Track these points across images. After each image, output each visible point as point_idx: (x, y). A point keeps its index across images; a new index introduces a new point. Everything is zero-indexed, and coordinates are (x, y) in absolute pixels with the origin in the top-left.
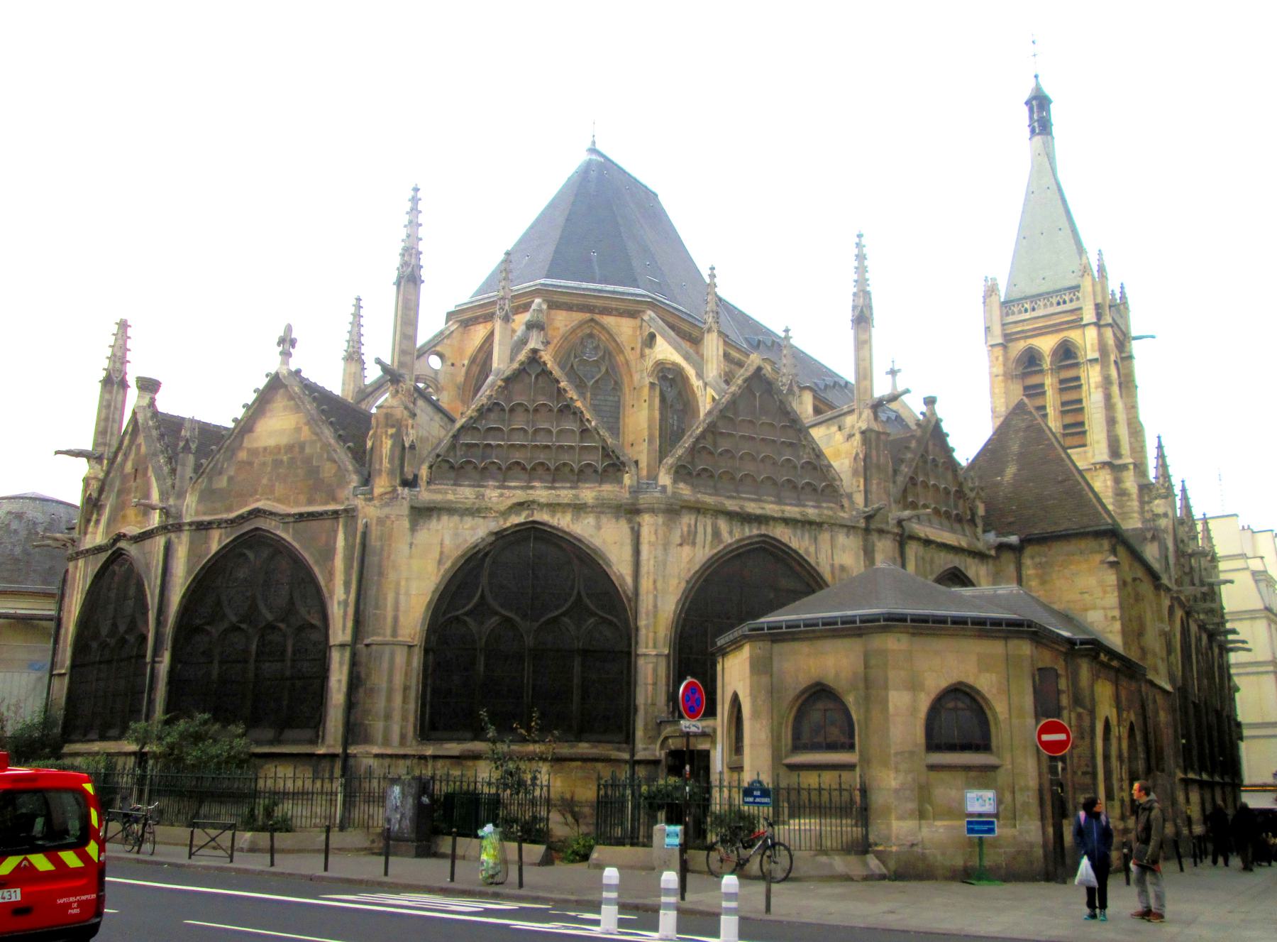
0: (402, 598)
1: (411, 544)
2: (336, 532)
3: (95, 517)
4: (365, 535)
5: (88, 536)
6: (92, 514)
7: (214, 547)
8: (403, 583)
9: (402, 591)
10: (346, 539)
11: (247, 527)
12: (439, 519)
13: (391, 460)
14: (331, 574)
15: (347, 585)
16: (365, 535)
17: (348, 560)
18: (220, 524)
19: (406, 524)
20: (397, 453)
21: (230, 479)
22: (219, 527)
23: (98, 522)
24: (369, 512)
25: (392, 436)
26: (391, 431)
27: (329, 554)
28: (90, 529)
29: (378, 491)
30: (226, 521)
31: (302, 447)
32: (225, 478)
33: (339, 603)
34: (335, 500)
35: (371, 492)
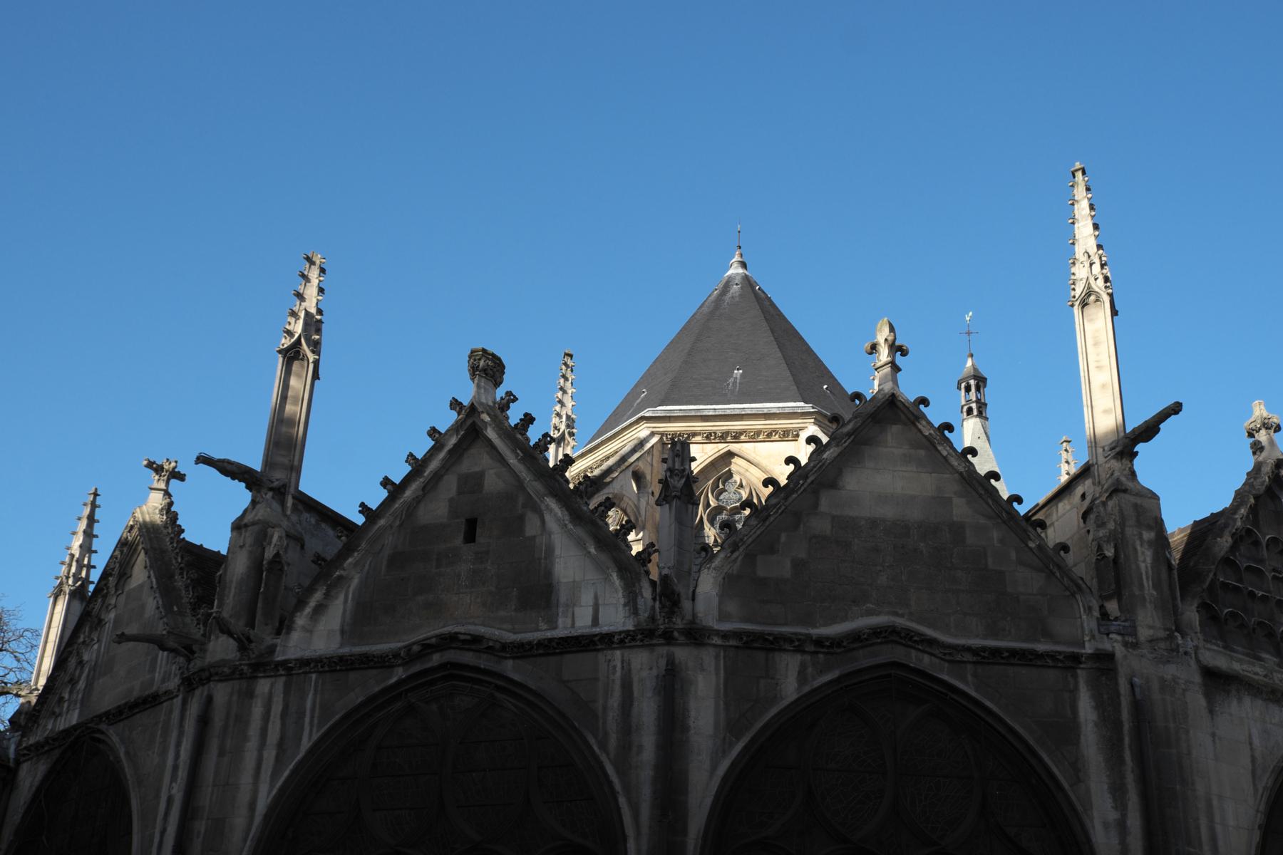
0: (1219, 828)
1: (1213, 735)
2: (1074, 692)
3: (318, 596)
4: (1138, 708)
5: (295, 636)
6: (310, 590)
7: (790, 689)
8: (1215, 802)
9: (1217, 819)
10: (1099, 705)
11: (864, 659)
12: (1240, 700)
13: (1157, 586)
14: (1077, 770)
15: (1118, 791)
16: (1138, 708)
17: (1112, 747)
18: (797, 644)
19: (1202, 702)
20: (1164, 575)
21: (798, 565)
22: (799, 650)
23: (320, 609)
24: (1136, 666)
25: (1150, 543)
26: (1148, 535)
27: (1067, 732)
28: (301, 620)
29: (1144, 633)
30: (819, 642)
31: (958, 530)
32: (788, 564)
33: (1106, 825)
34: (1048, 635)
35: (1134, 634)
